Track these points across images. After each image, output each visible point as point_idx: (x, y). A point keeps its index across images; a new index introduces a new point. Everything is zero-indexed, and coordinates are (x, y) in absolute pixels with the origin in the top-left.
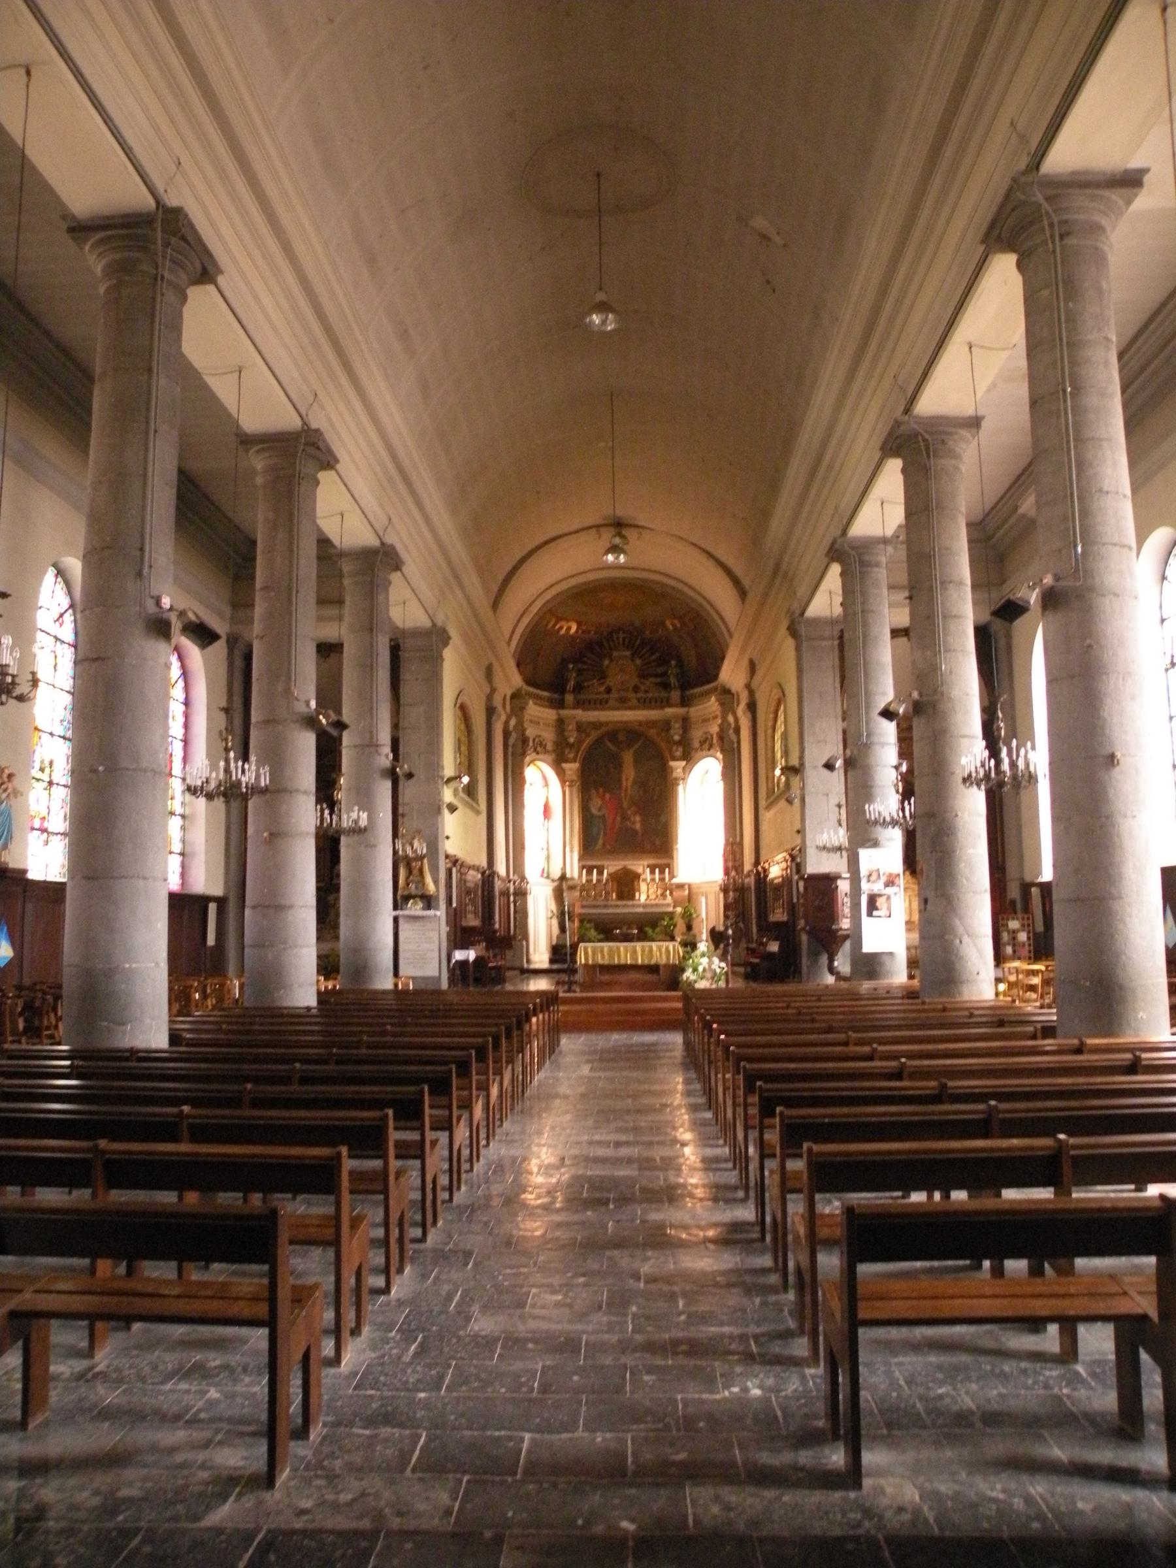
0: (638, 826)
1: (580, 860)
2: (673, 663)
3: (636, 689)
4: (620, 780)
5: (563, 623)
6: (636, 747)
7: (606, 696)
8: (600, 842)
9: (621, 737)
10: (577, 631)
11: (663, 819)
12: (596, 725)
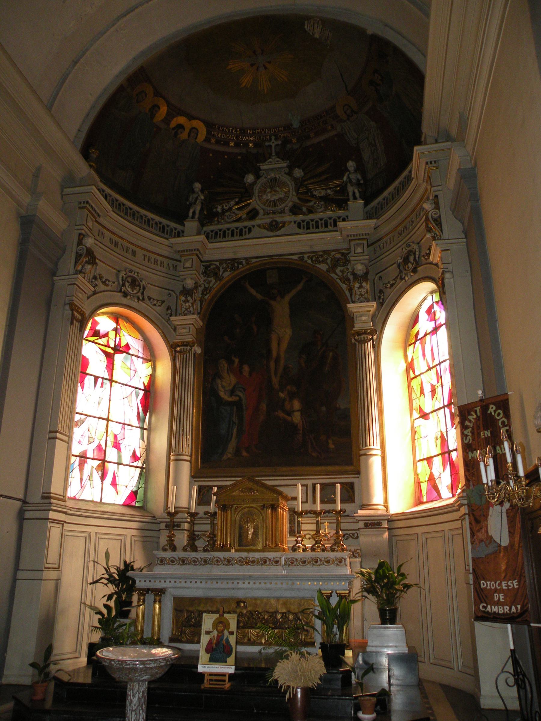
0: (297, 418)
1: (195, 476)
2: (351, 165)
3: (295, 210)
4: (268, 343)
5: (181, 120)
6: (294, 292)
7: (249, 224)
8: (233, 443)
9: (272, 278)
11: (341, 404)
12: (233, 263)
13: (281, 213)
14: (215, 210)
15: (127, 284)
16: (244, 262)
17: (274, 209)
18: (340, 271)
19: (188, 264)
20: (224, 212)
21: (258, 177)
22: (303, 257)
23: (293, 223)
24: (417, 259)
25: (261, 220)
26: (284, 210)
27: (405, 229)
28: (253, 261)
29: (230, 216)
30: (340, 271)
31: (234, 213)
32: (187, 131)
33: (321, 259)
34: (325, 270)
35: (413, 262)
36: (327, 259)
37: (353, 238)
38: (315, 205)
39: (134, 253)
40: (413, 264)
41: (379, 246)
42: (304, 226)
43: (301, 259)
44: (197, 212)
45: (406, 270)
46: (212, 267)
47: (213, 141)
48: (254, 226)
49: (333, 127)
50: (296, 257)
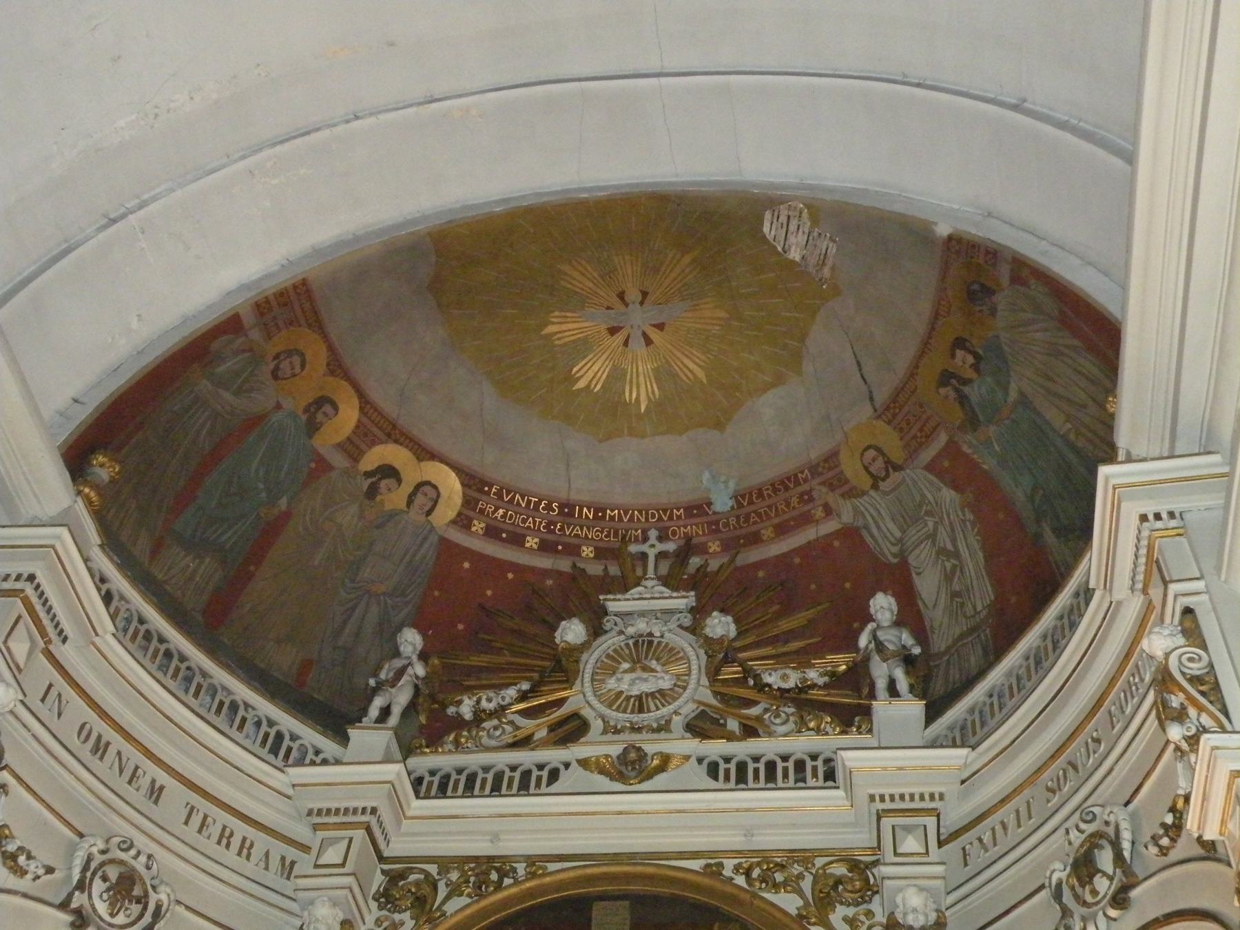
2: (883, 605)
3: (701, 727)
7: (554, 756)
10: (462, 522)
12: (484, 871)
13: (659, 730)
14: (451, 710)
15: (98, 886)
16: (521, 868)
17: (636, 718)
18: (845, 919)
19: (333, 855)
20: (480, 717)
21: (596, 631)
22: (721, 865)
23: (693, 760)
24: (1127, 854)
25: (592, 748)
26: (668, 722)
27: (1071, 771)
28: (552, 867)
29: (496, 728)
30: (845, 919)
31: (511, 723)
32: (407, 488)
33: (779, 877)
34: (794, 912)
35: (1109, 869)
36: (800, 877)
37: (888, 805)
38: (766, 716)
39: (156, 793)
40: (1111, 879)
41: (980, 840)
42: (727, 771)
43: (714, 871)
44: (396, 711)
45: (1085, 904)
46: (412, 878)
47: (478, 526)
48: (567, 765)
49: (828, 511)
50: (696, 865)
